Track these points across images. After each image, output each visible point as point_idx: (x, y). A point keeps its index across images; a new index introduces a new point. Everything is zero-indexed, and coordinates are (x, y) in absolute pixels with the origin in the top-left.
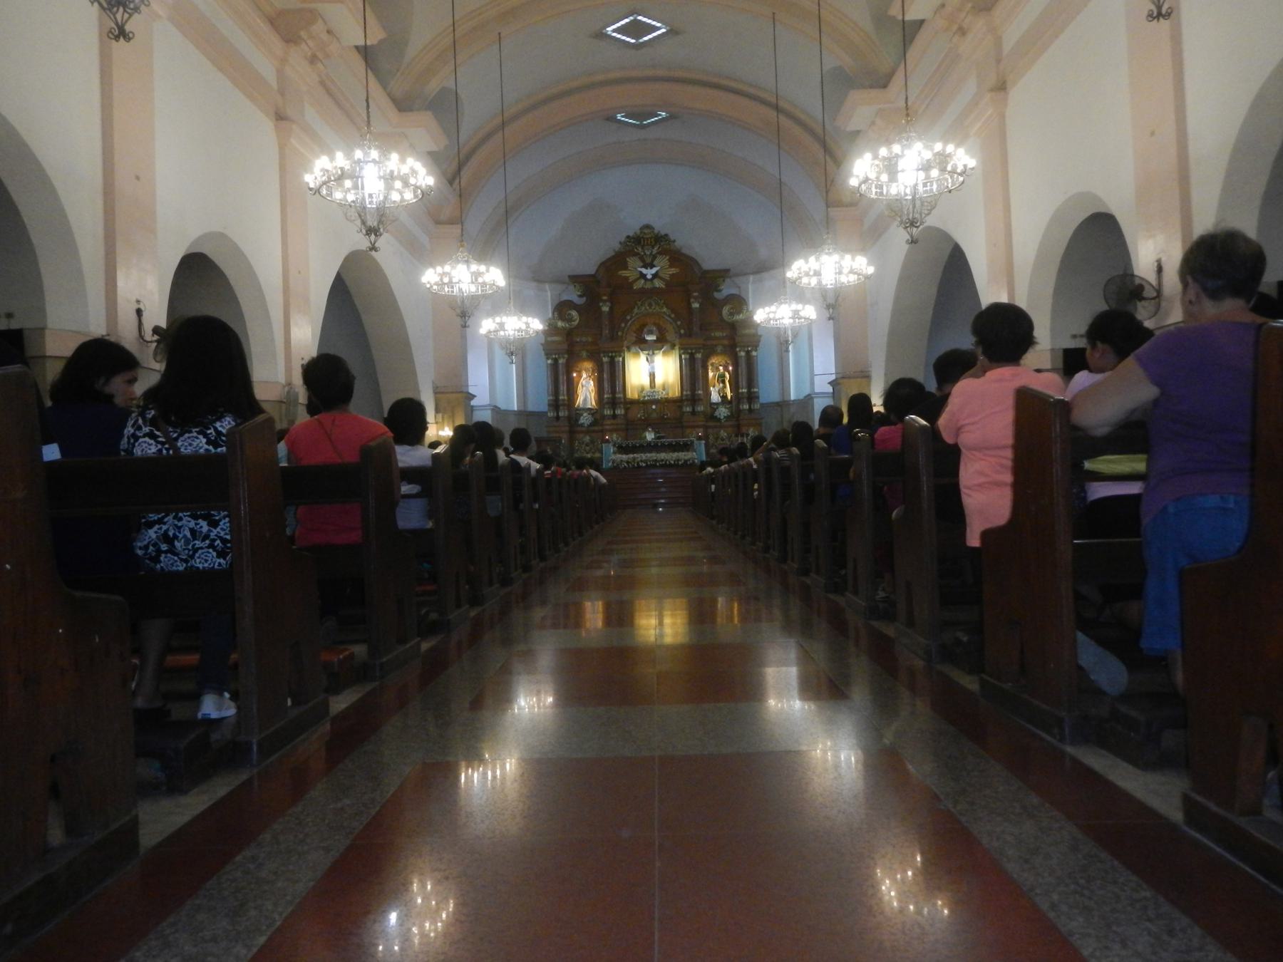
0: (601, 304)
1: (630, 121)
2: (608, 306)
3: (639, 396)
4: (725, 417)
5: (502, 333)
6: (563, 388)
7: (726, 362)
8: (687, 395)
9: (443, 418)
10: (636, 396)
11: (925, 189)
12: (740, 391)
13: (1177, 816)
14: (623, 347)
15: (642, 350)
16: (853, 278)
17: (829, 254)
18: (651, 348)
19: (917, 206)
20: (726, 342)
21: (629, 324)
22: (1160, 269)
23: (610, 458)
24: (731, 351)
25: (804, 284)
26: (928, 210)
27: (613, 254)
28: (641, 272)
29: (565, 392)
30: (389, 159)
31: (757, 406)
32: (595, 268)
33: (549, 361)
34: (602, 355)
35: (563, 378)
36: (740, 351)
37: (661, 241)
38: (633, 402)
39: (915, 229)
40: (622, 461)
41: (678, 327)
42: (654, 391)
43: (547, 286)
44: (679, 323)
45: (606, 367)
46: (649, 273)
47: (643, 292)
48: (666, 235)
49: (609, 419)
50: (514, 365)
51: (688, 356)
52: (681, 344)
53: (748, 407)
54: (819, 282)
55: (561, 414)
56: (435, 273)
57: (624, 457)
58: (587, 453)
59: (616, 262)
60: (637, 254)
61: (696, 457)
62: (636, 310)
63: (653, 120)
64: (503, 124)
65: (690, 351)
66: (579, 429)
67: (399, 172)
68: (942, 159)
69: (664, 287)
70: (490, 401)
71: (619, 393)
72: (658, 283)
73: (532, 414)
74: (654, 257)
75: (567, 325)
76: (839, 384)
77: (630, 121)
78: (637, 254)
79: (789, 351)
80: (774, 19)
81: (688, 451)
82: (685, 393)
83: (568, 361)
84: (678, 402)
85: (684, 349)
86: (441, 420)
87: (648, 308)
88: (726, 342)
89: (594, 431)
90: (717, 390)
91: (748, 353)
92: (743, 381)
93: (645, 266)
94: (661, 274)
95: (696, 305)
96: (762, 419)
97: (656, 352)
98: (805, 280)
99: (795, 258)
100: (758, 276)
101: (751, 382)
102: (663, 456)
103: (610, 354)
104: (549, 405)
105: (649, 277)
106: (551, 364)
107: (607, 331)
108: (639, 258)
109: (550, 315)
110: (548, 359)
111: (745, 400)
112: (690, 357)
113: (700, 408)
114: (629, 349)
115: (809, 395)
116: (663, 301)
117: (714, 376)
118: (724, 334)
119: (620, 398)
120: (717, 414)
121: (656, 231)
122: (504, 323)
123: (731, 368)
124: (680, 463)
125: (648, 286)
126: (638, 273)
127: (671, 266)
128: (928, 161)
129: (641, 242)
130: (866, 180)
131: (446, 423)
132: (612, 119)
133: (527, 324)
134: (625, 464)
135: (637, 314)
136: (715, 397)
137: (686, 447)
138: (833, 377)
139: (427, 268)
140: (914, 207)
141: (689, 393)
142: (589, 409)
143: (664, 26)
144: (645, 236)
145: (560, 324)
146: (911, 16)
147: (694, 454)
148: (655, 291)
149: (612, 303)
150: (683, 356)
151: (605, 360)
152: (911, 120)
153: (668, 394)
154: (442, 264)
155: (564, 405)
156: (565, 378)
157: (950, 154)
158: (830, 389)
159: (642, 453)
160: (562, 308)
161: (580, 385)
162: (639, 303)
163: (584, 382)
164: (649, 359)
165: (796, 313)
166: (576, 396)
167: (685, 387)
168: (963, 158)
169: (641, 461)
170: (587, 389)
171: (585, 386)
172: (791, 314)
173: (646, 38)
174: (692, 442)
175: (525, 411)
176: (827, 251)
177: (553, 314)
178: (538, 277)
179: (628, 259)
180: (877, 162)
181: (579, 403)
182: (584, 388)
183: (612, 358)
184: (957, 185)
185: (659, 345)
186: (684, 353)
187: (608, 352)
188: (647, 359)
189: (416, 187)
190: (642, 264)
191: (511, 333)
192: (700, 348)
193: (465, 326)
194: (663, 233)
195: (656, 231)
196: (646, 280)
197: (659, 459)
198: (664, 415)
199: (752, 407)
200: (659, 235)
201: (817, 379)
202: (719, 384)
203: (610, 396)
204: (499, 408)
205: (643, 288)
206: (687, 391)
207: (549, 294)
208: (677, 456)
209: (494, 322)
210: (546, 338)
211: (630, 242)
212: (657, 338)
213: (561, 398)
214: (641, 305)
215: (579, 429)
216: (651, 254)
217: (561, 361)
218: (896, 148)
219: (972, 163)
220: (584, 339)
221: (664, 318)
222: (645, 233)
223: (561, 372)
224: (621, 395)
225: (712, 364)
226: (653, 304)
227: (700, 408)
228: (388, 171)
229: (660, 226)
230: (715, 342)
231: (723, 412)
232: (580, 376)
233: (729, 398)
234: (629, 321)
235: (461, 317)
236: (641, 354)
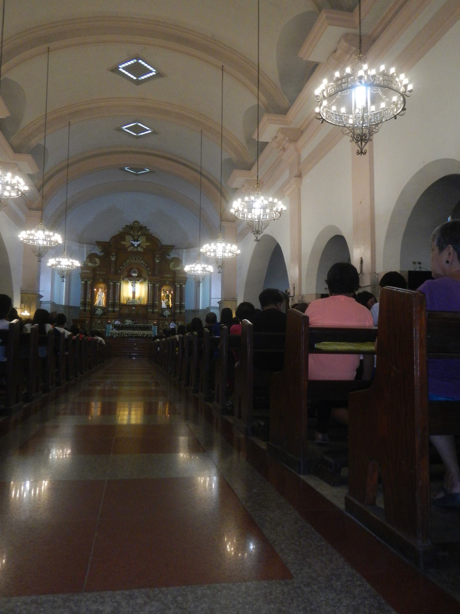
0: (111, 257)
1: (132, 171)
2: (114, 258)
3: (126, 302)
4: (168, 315)
5: (59, 266)
6: (89, 296)
7: (170, 289)
8: (150, 304)
9: (25, 306)
10: (125, 302)
11: (263, 217)
12: (176, 303)
13: (342, 506)
14: (120, 278)
15: (130, 280)
16: (230, 255)
17: (220, 243)
18: (134, 280)
19: (260, 224)
20: (171, 280)
22: (362, 262)
23: (110, 332)
24: (173, 284)
25: (208, 255)
26: (265, 227)
27: (119, 233)
28: (132, 244)
29: (90, 298)
30: (6, 175)
31: (184, 311)
32: (109, 239)
33: (83, 282)
34: (110, 281)
35: (89, 291)
36: (177, 284)
37: (143, 229)
39: (258, 235)
40: (116, 333)
41: (148, 271)
42: (134, 301)
43: (85, 245)
44: (149, 269)
45: (111, 287)
46: (136, 244)
47: (132, 252)
48: (146, 227)
50: (64, 283)
51: (152, 285)
52: (148, 279)
53: (179, 311)
54: (215, 255)
55: (87, 308)
56: (26, 233)
57: (117, 332)
58: (99, 328)
59: (120, 237)
60: (130, 234)
61: (152, 334)
62: (128, 261)
63: (142, 172)
64: (68, 166)
65: (153, 283)
66: (96, 316)
67: (11, 182)
68: (272, 205)
69: (143, 251)
70: (51, 299)
71: (117, 300)
72: (140, 249)
73: (71, 307)
74: (139, 237)
75: (93, 265)
76: (222, 303)
77: (132, 171)
79: (200, 287)
80: (202, 133)
81: (149, 330)
82: (149, 302)
83: (93, 282)
84: (145, 307)
85: (150, 281)
86: (23, 307)
87: (134, 260)
89: (103, 318)
90: (165, 302)
91: (181, 285)
92: (178, 299)
93: (134, 241)
94: (141, 245)
95: (157, 261)
97: (136, 282)
98: (208, 254)
99: (205, 243)
101: (181, 299)
102: (136, 332)
104: (81, 304)
105: (136, 246)
106: (84, 284)
107: (113, 270)
108: (131, 236)
109: (85, 260)
110: (82, 281)
111: (178, 308)
112: (153, 285)
113: (156, 310)
114: (123, 279)
115: (208, 307)
116: (141, 258)
117: (164, 296)
118: (170, 276)
119: (117, 302)
120: (164, 313)
121: (140, 224)
122: (61, 261)
123: (172, 292)
124: (144, 336)
125: (135, 250)
127: (147, 242)
128: (266, 205)
130: (237, 211)
131: (26, 309)
132: (123, 169)
133: (72, 263)
134: (118, 335)
135: (129, 263)
136: (164, 305)
137: (148, 328)
138: (220, 300)
139: (22, 230)
140: (259, 225)
141: (151, 302)
142: (101, 307)
143: (150, 130)
145: (90, 264)
146: (263, 139)
147: (152, 332)
148: (138, 253)
150: (150, 285)
151: (111, 283)
152: (259, 186)
153: (141, 302)
154: (31, 229)
155: (89, 304)
156: (90, 291)
157: (276, 203)
158: (218, 305)
159: (126, 330)
160: (91, 257)
161: (97, 295)
163: (100, 294)
164: (133, 285)
165: (204, 268)
166: (95, 300)
167: (150, 300)
168: (281, 206)
169: (125, 334)
170: (101, 296)
171: (100, 296)
172: (201, 269)
173: (141, 134)
174: (151, 326)
175: (68, 306)
176: (219, 241)
177: (87, 259)
178: (81, 241)
179: (126, 236)
180: (243, 203)
181: (96, 305)
182: (100, 297)
183: (115, 283)
184: (278, 217)
185: (138, 278)
186: (150, 283)
188: (132, 285)
189: (19, 190)
190: (132, 239)
191: (64, 267)
192: (158, 282)
193: (40, 261)
194: (144, 225)
197: (134, 333)
198: (138, 312)
199: (181, 312)
200: (142, 226)
201: (212, 300)
202: (166, 299)
203: (113, 301)
204: (55, 303)
205: (132, 251)
206: (150, 302)
207: (85, 250)
208: (144, 333)
209: (55, 261)
210: (82, 271)
211: (127, 228)
212: (137, 275)
214: (131, 259)
215: (96, 316)
216: (137, 235)
217: (89, 283)
218: (252, 198)
219: (285, 208)
220: (101, 273)
221: (142, 266)
222: (135, 225)
223: (88, 288)
224: (118, 301)
225: (163, 290)
226: (137, 258)
227: (156, 310)
228: (5, 181)
229: (143, 221)
230: (165, 279)
231: (167, 313)
232: (98, 291)
233: (171, 306)
234: (124, 266)
235: (38, 256)
236: (129, 282)
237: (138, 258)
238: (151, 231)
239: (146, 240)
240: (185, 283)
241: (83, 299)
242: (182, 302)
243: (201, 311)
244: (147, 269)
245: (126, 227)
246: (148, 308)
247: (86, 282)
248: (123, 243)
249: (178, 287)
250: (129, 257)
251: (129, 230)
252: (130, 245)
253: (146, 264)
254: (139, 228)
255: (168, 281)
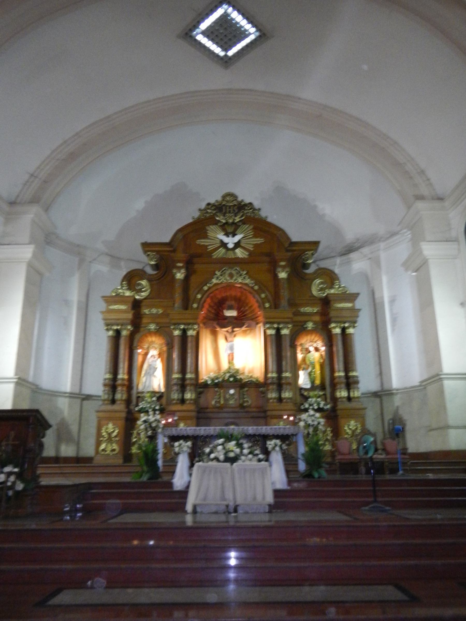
12: (337, 374)
21: (205, 296)
27: (191, 221)
28: (222, 241)
33: (111, 333)
36: (334, 328)
37: (244, 209)
38: (205, 385)
43: (122, 263)
44: (263, 296)
46: (231, 241)
48: (251, 204)
49: (176, 404)
60: (216, 223)
62: (214, 281)
65: (276, 326)
72: (239, 253)
73: (88, 397)
78: (218, 222)
82: (270, 375)
85: (268, 322)
87: (228, 278)
88: (317, 318)
93: (227, 235)
94: (242, 244)
95: (283, 275)
96: (365, 409)
97: (235, 329)
100: (344, 258)
103: (182, 327)
104: (105, 385)
105: (231, 246)
106: (112, 337)
108: (221, 226)
110: (108, 330)
111: (343, 386)
116: (245, 272)
121: (240, 199)
125: (230, 255)
126: (218, 242)
127: (255, 236)
129: (222, 211)
141: (275, 375)
144: (228, 204)
145: (128, 293)
148: (237, 262)
149: (187, 269)
162: (218, 273)
183: (184, 331)
186: (269, 328)
187: (179, 324)
188: (226, 339)
194: (247, 201)
195: (240, 199)
196: (228, 249)
198: (244, 402)
200: (243, 203)
204: (37, 386)
205: (222, 258)
213: (120, 376)
214: (221, 275)
217: (124, 333)
220: (154, 311)
222: (228, 201)
225: (301, 345)
226: (234, 272)
237: (237, 273)
238: (263, 214)
239: (252, 233)
240: (355, 322)
241: (110, 373)
242: (353, 371)
243: (397, 393)
244: (260, 296)
245: (207, 207)
246: (268, 390)
247: (118, 332)
248: (204, 242)
249: (337, 334)
250: (217, 272)
251: (214, 212)
252: (219, 245)
253: (256, 285)
254: (236, 207)
255: (312, 321)
